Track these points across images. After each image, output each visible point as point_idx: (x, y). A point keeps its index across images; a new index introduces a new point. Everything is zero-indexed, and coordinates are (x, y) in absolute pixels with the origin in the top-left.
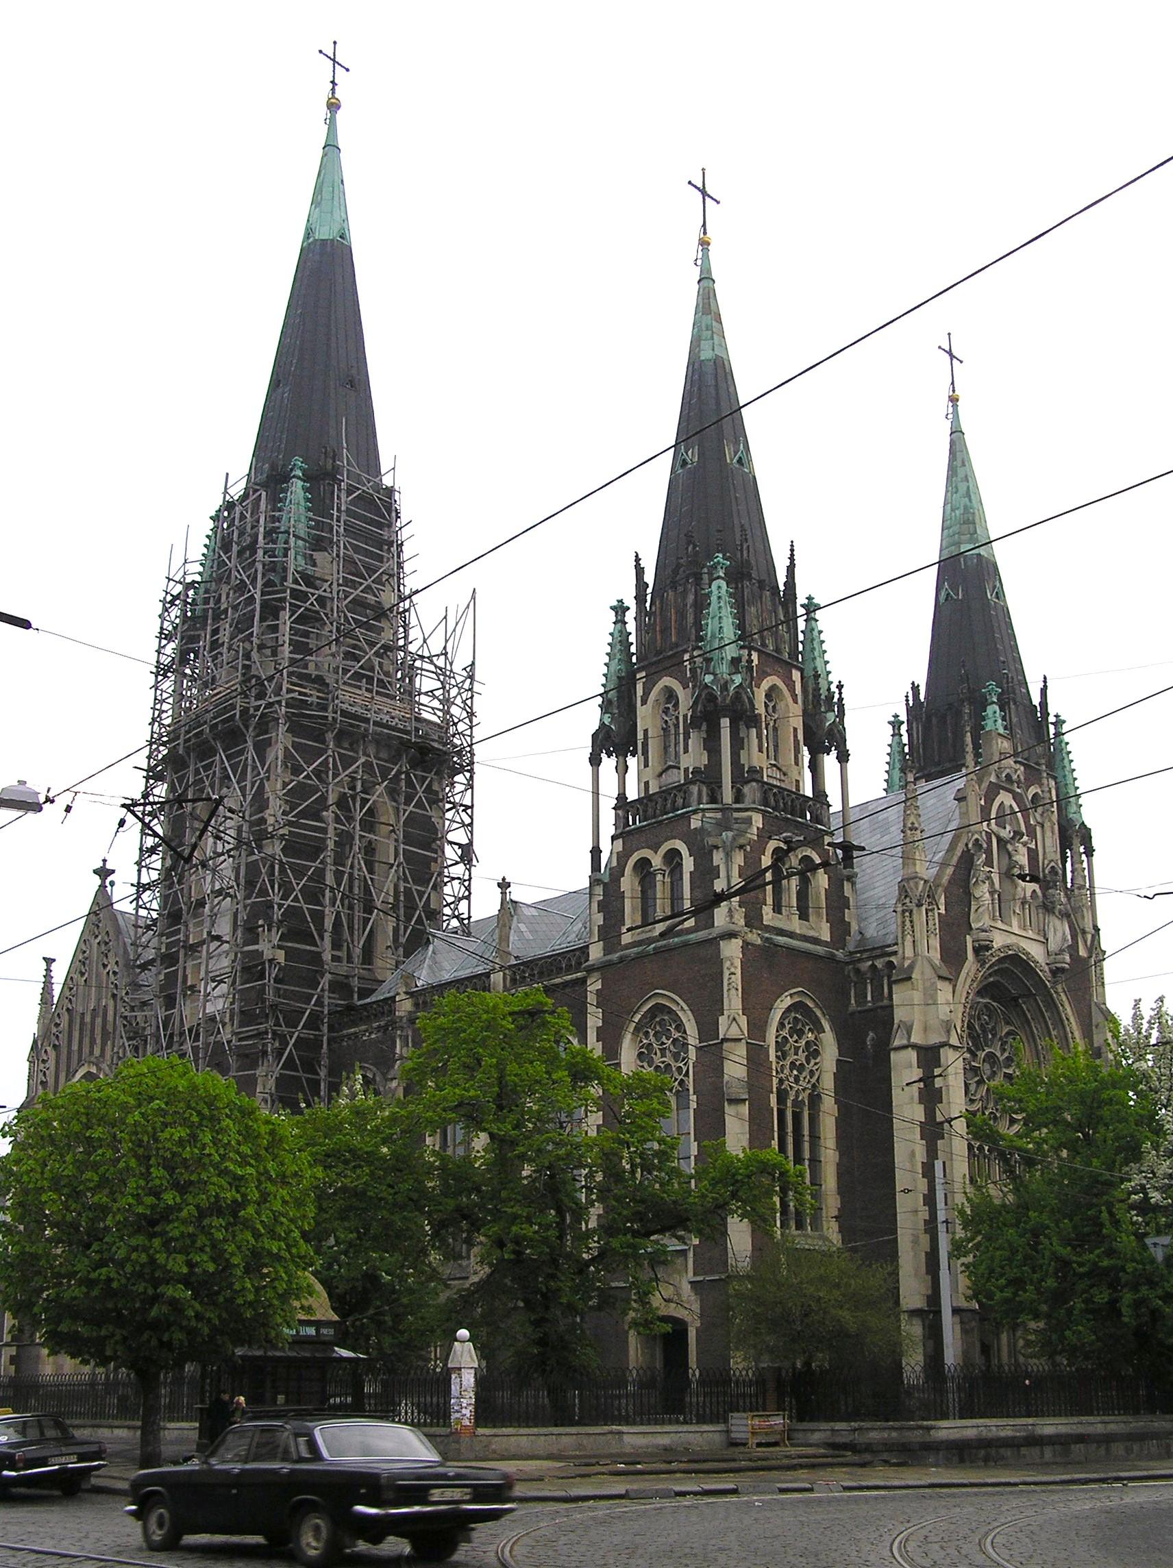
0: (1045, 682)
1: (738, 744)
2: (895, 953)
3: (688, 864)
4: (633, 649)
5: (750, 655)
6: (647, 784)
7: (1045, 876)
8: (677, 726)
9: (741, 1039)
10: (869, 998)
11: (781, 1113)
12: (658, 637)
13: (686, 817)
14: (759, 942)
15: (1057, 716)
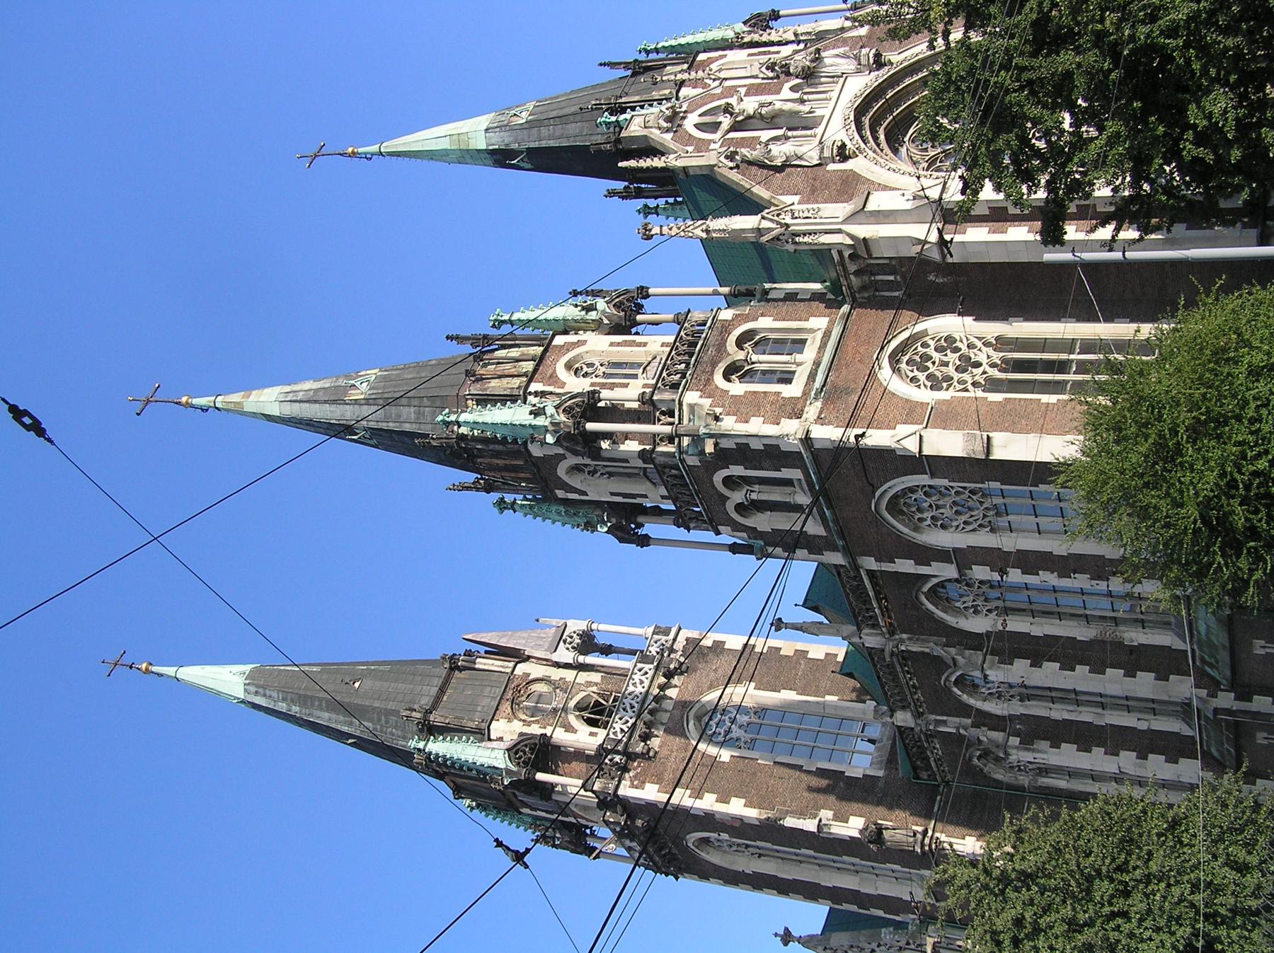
0: (605, 64)
1: (615, 413)
2: (840, 253)
3: (737, 470)
5: (530, 393)
10: (892, 278)
14: (819, 404)
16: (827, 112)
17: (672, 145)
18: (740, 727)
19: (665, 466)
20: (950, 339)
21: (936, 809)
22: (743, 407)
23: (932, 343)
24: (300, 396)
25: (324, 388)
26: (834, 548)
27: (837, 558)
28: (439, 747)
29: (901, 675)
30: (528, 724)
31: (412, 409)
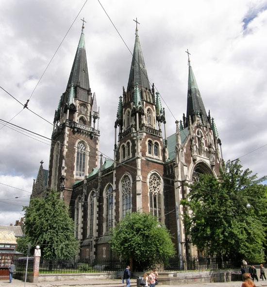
1: (140, 119)
3: (131, 144)
16: (202, 156)
19: (130, 130)
28: (72, 89)
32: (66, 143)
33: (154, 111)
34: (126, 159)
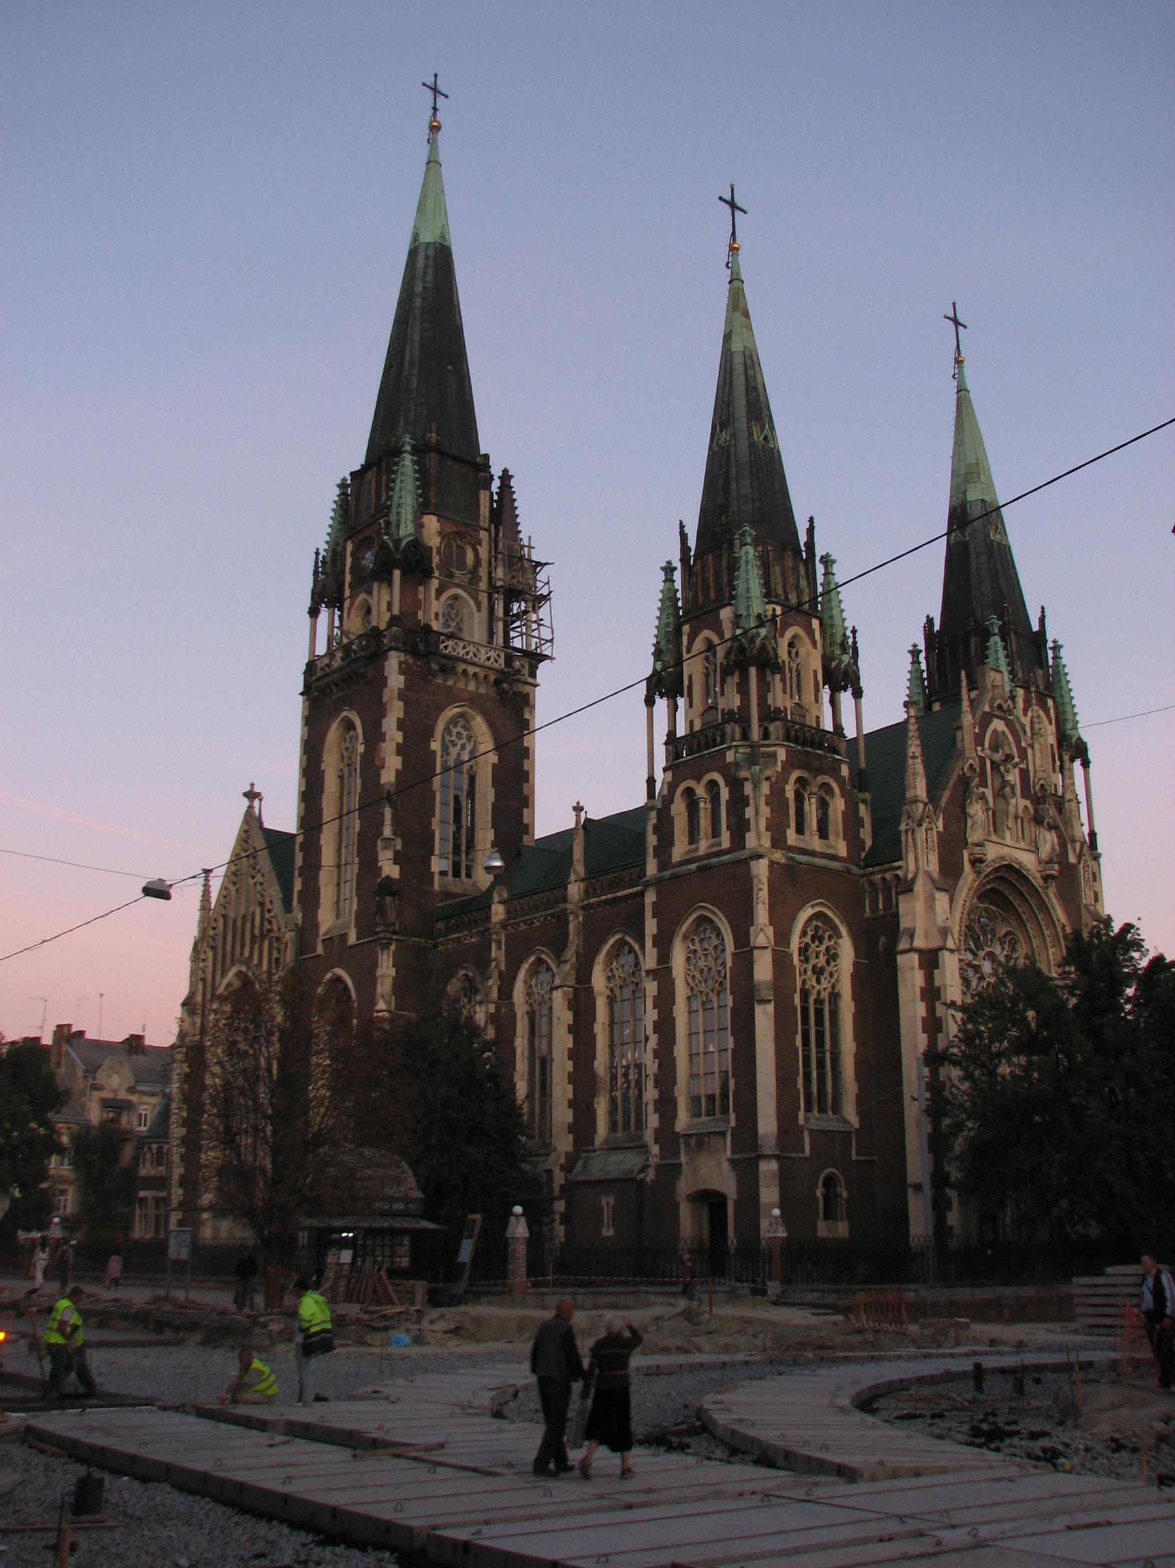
1: (765, 688)
2: (900, 868)
3: (725, 794)
4: (680, 604)
5: (774, 610)
6: (691, 722)
7: (1035, 793)
8: (715, 672)
9: (766, 948)
10: (881, 907)
11: (805, 1011)
12: (700, 596)
13: (722, 753)
14: (783, 861)
15: (1055, 642)
17: (979, 713)
18: (459, 755)
20: (834, 957)
21: (414, 939)
22: (776, 800)
23: (832, 943)
24: (751, 373)
25: (759, 396)
26: (662, 867)
27: (652, 868)
29: (543, 913)
30: (438, 552)
31: (749, 491)
32: (390, 725)
33: (815, 647)
34: (703, 846)
